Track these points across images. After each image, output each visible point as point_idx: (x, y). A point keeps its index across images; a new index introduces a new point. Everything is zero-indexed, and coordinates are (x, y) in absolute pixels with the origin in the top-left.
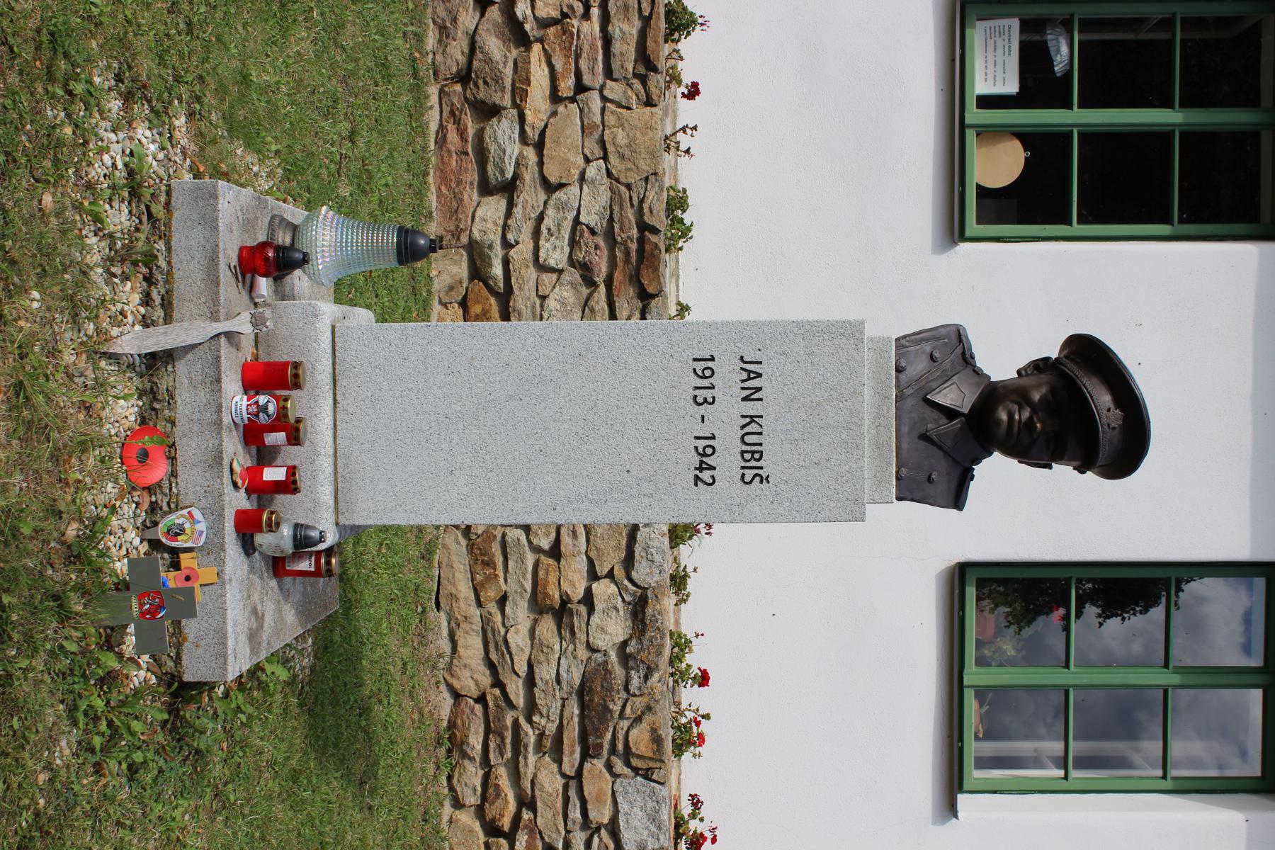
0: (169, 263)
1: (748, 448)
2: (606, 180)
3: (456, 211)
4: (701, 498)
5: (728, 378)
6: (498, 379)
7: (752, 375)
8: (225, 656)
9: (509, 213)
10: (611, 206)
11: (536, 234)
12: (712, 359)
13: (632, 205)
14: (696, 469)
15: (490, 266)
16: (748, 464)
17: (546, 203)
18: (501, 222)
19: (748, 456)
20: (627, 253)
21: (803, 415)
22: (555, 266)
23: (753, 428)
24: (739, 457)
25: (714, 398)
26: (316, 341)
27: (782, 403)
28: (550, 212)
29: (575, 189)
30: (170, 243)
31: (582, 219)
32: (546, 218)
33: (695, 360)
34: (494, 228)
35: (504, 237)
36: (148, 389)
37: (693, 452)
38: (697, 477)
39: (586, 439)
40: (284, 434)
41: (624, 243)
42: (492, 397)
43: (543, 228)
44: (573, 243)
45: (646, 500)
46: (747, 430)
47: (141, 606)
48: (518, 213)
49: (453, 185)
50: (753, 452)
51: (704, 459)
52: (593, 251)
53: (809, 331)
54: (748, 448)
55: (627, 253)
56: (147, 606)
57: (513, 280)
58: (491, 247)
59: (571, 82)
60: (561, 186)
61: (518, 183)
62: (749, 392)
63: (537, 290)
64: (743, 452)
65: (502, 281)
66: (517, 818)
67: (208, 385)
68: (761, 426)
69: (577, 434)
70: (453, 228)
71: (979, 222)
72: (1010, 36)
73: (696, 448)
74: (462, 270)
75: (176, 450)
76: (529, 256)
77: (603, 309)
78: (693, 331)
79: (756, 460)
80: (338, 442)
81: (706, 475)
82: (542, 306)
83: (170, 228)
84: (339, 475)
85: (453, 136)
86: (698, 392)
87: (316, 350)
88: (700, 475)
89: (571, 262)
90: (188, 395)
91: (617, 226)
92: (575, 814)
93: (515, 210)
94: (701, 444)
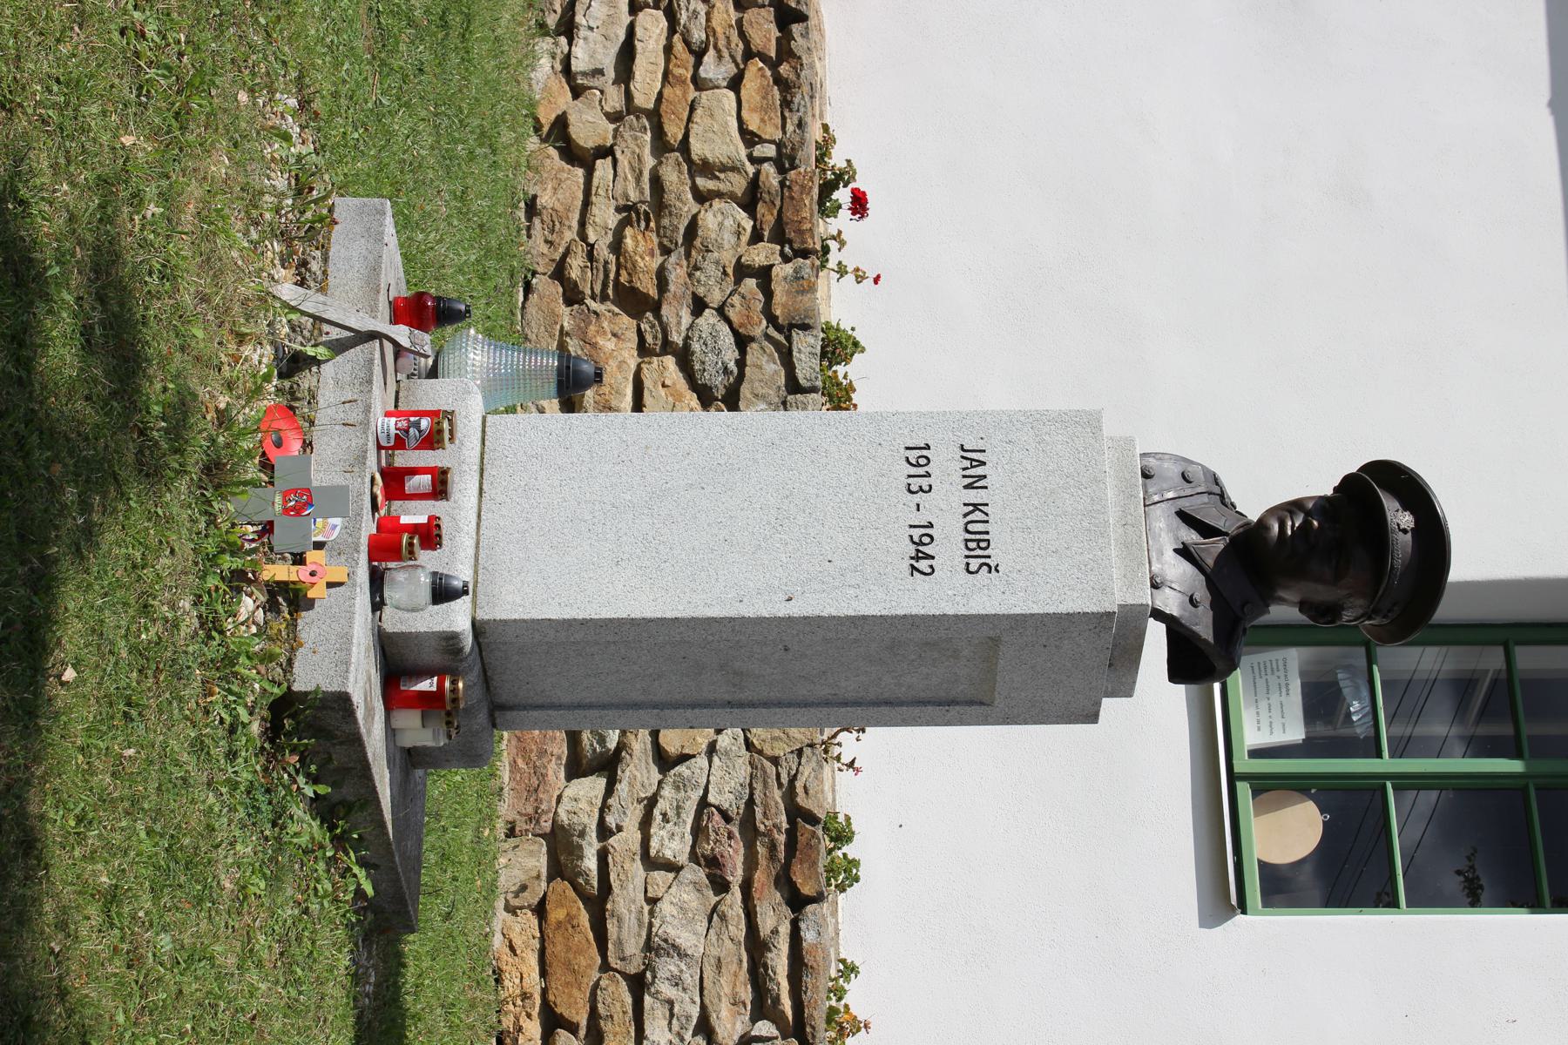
0: (325, 273)
1: (973, 537)
2: (743, 751)
3: (536, 790)
4: (918, 588)
5: (946, 467)
6: (676, 468)
7: (974, 463)
8: (347, 663)
10: (751, 785)
11: (645, 824)
12: (928, 447)
13: (780, 785)
14: (912, 558)
15: (581, 857)
16: (972, 553)
17: (660, 783)
18: (599, 803)
19: (972, 545)
20: (772, 847)
21: (1036, 503)
22: (672, 858)
23: (977, 516)
24: (963, 547)
25: (930, 486)
26: (466, 417)
27: (1011, 491)
28: (667, 792)
29: (702, 761)
30: (327, 254)
31: (711, 799)
32: (661, 800)
33: (907, 448)
34: (588, 809)
35: (601, 823)
36: (287, 389)
37: (908, 540)
38: (913, 567)
39: (779, 528)
40: (430, 476)
41: (768, 834)
42: (668, 485)
43: (656, 812)
44: (698, 831)
45: (852, 592)
46: (970, 518)
47: (285, 502)
48: (623, 790)
49: (534, 756)
50: (979, 541)
51: (920, 548)
52: (724, 839)
53: (1036, 420)
54: (973, 537)
55: (772, 847)
56: (292, 503)
57: (613, 877)
58: (582, 834)
60: (684, 758)
61: (623, 754)
62: (971, 480)
63: (646, 891)
64: (967, 541)
65: (596, 879)
67: (357, 386)
68: (987, 514)
69: (769, 523)
70: (530, 810)
71: (1263, 907)
72: (1286, 672)
73: (911, 537)
74: (541, 863)
75: (312, 448)
76: (636, 847)
77: (738, 915)
78: (904, 421)
79: (981, 548)
80: (482, 532)
81: (923, 565)
82: (652, 913)
83: (329, 240)
84: (481, 566)
86: (911, 480)
87: (465, 425)
88: (916, 565)
89: (694, 857)
90: (332, 395)
91: (759, 811)
93: (618, 786)
94: (916, 533)
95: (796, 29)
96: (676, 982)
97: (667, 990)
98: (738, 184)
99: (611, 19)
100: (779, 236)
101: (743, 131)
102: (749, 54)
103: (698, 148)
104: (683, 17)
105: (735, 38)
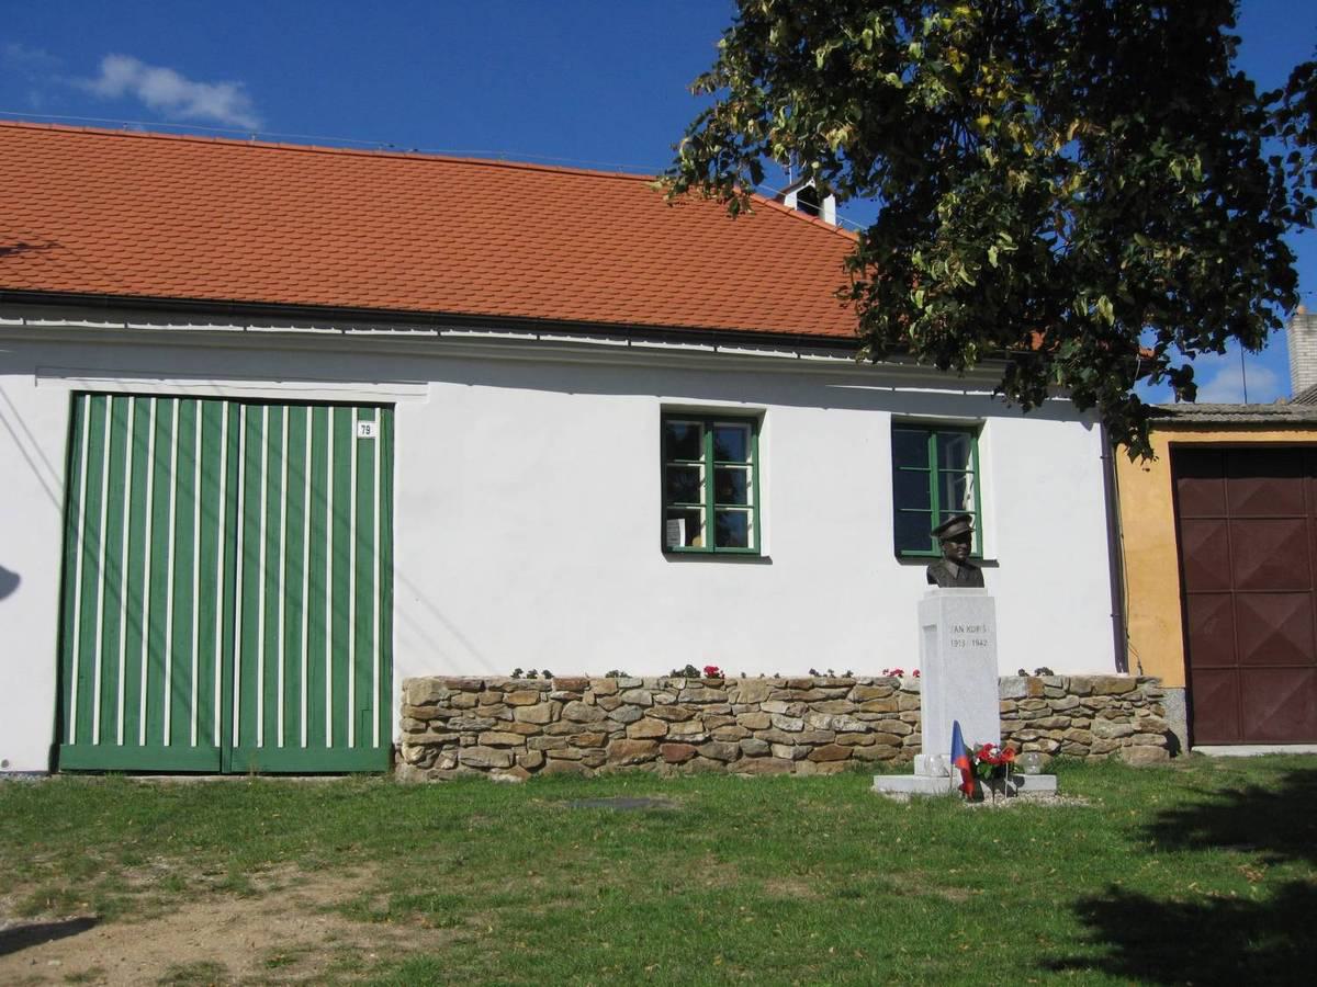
9: (778, 743)
11: (790, 731)
28: (780, 726)
44: (793, 716)
55: (798, 694)
59: (729, 717)
60: (771, 722)
66: (1015, 739)
85: (751, 767)
92: (1013, 715)
95: (487, 685)
96: (839, 722)
97: (842, 724)
98: (558, 704)
99: (485, 753)
100: (582, 691)
101: (535, 704)
102: (501, 702)
103: (545, 719)
104: (484, 726)
105: (494, 706)
